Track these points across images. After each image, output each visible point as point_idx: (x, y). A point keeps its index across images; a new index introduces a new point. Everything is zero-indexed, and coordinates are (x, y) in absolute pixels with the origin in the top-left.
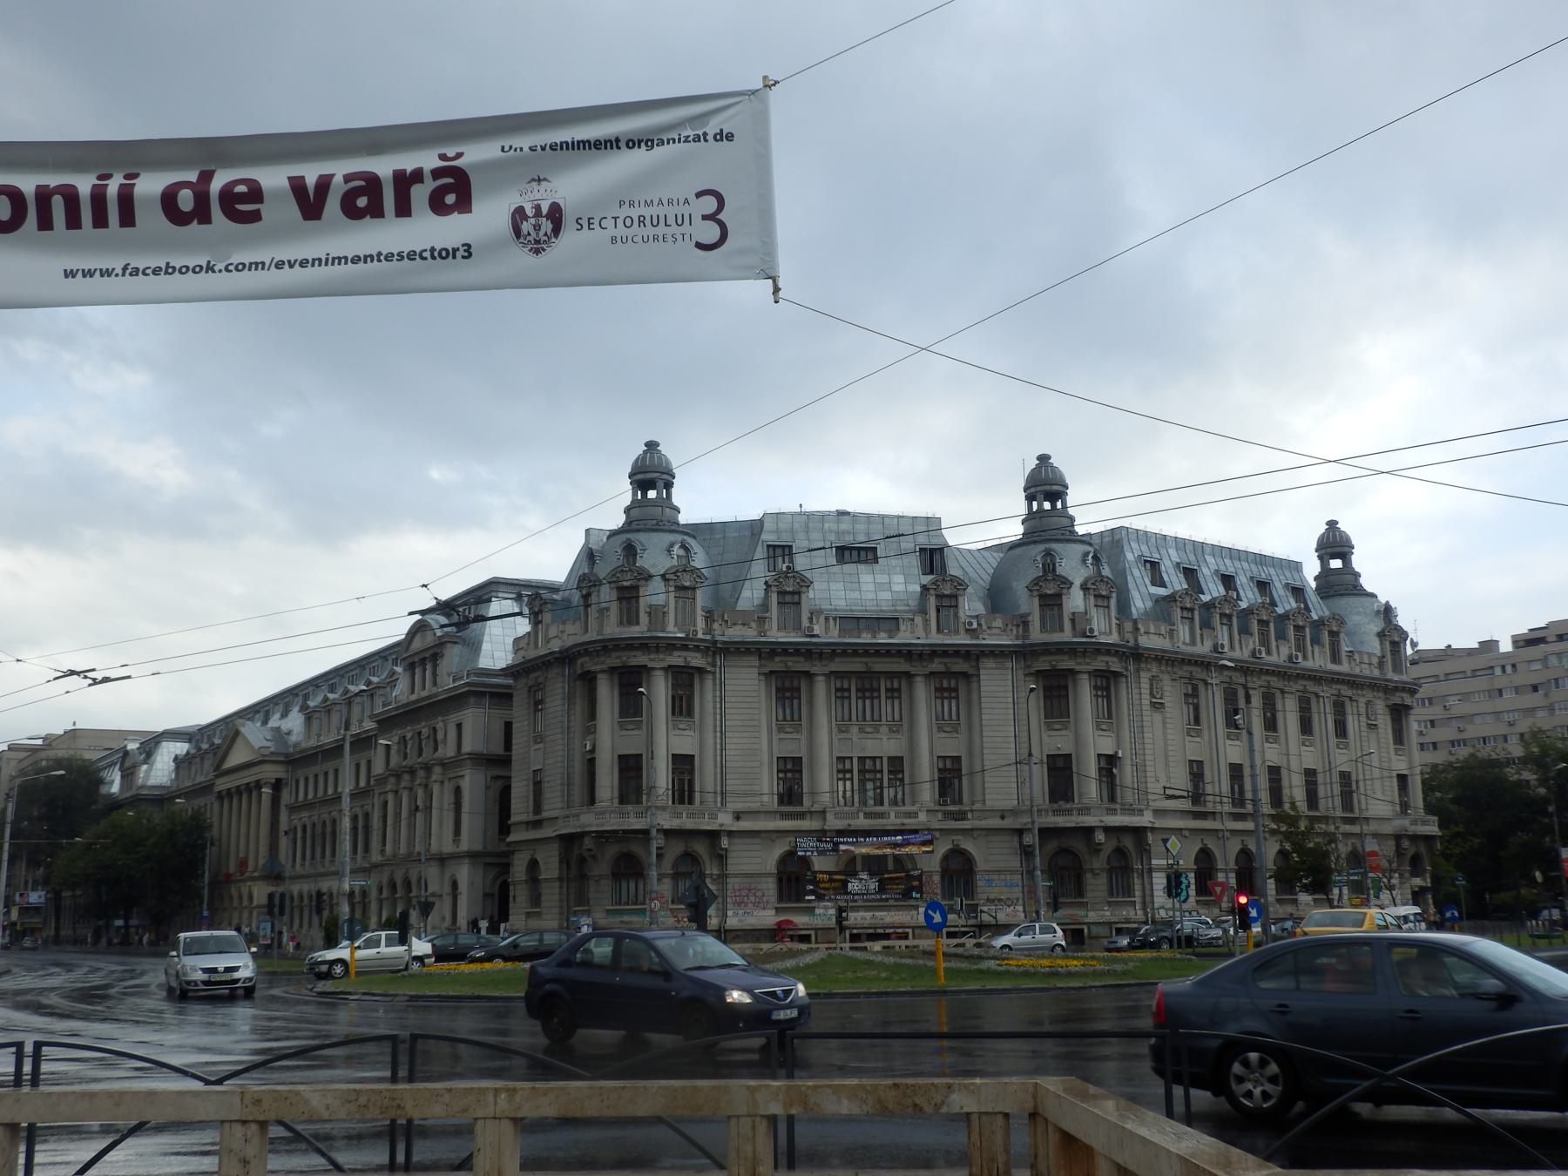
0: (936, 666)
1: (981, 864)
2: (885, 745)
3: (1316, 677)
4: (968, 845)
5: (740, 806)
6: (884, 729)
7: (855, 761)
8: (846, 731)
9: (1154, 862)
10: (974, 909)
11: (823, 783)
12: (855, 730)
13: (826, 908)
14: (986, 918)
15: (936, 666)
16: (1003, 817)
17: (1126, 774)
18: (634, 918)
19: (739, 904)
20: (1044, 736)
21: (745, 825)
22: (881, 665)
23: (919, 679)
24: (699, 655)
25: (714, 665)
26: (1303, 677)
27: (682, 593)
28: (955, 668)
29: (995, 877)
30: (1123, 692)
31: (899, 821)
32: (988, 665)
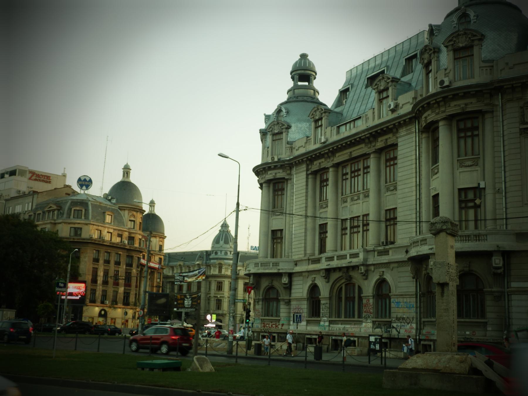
1: (394, 291)
2: (357, 209)
4: (388, 277)
8: (346, 202)
10: (388, 325)
14: (394, 332)
21: (298, 269)
24: (281, 171)
25: (290, 174)
29: (401, 300)
32: (402, 132)
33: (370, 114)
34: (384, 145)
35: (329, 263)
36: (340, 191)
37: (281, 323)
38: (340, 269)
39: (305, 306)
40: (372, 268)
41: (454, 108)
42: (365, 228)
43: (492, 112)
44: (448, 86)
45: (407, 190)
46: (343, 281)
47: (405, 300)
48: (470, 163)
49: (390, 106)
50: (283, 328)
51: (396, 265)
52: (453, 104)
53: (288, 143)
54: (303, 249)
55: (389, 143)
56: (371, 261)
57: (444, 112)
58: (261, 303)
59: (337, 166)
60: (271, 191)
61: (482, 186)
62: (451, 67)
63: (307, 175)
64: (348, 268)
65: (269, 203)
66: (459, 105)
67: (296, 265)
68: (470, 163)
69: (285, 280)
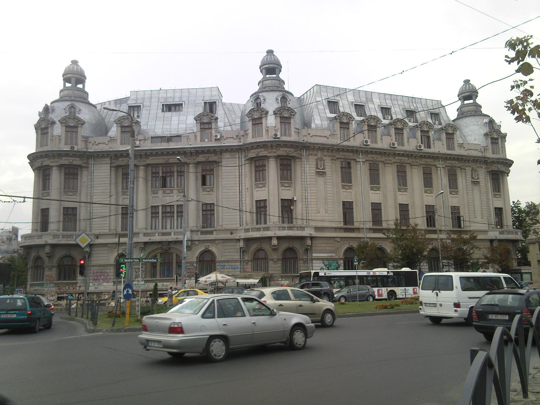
0: (201, 158)
1: (219, 258)
3: (436, 157)
4: (213, 249)
5: (97, 232)
6: (175, 191)
7: (160, 208)
8: (157, 193)
9: (314, 255)
11: (141, 220)
12: (160, 192)
13: (138, 281)
15: (201, 158)
16: (232, 233)
17: (299, 210)
18: (40, 288)
19: (96, 280)
20: (254, 191)
22: (173, 160)
23: (191, 165)
24: (78, 159)
26: (425, 157)
27: (69, 129)
28: (211, 159)
29: (227, 264)
30: (298, 168)
31: (176, 237)
32: (227, 155)
33: (192, 137)
34: (204, 160)
35: (149, 238)
36: (150, 185)
37: (78, 285)
38: (160, 243)
39: (112, 271)
40: (197, 243)
41: (282, 152)
42: (179, 214)
43: (301, 159)
44: (278, 138)
45: (231, 194)
46: (158, 251)
47: (230, 264)
48: (287, 185)
49: (216, 136)
50: (81, 289)
51: (221, 241)
52: (281, 149)
53: (83, 137)
54: (108, 225)
55: (210, 160)
56: (197, 237)
57: (275, 152)
58: (54, 269)
59: (147, 165)
60: (63, 174)
61: (295, 199)
62: (279, 126)
63: (111, 167)
64: (169, 242)
65: (61, 184)
66: (286, 151)
67: (97, 238)
68: (287, 185)
69: (48, 249)
